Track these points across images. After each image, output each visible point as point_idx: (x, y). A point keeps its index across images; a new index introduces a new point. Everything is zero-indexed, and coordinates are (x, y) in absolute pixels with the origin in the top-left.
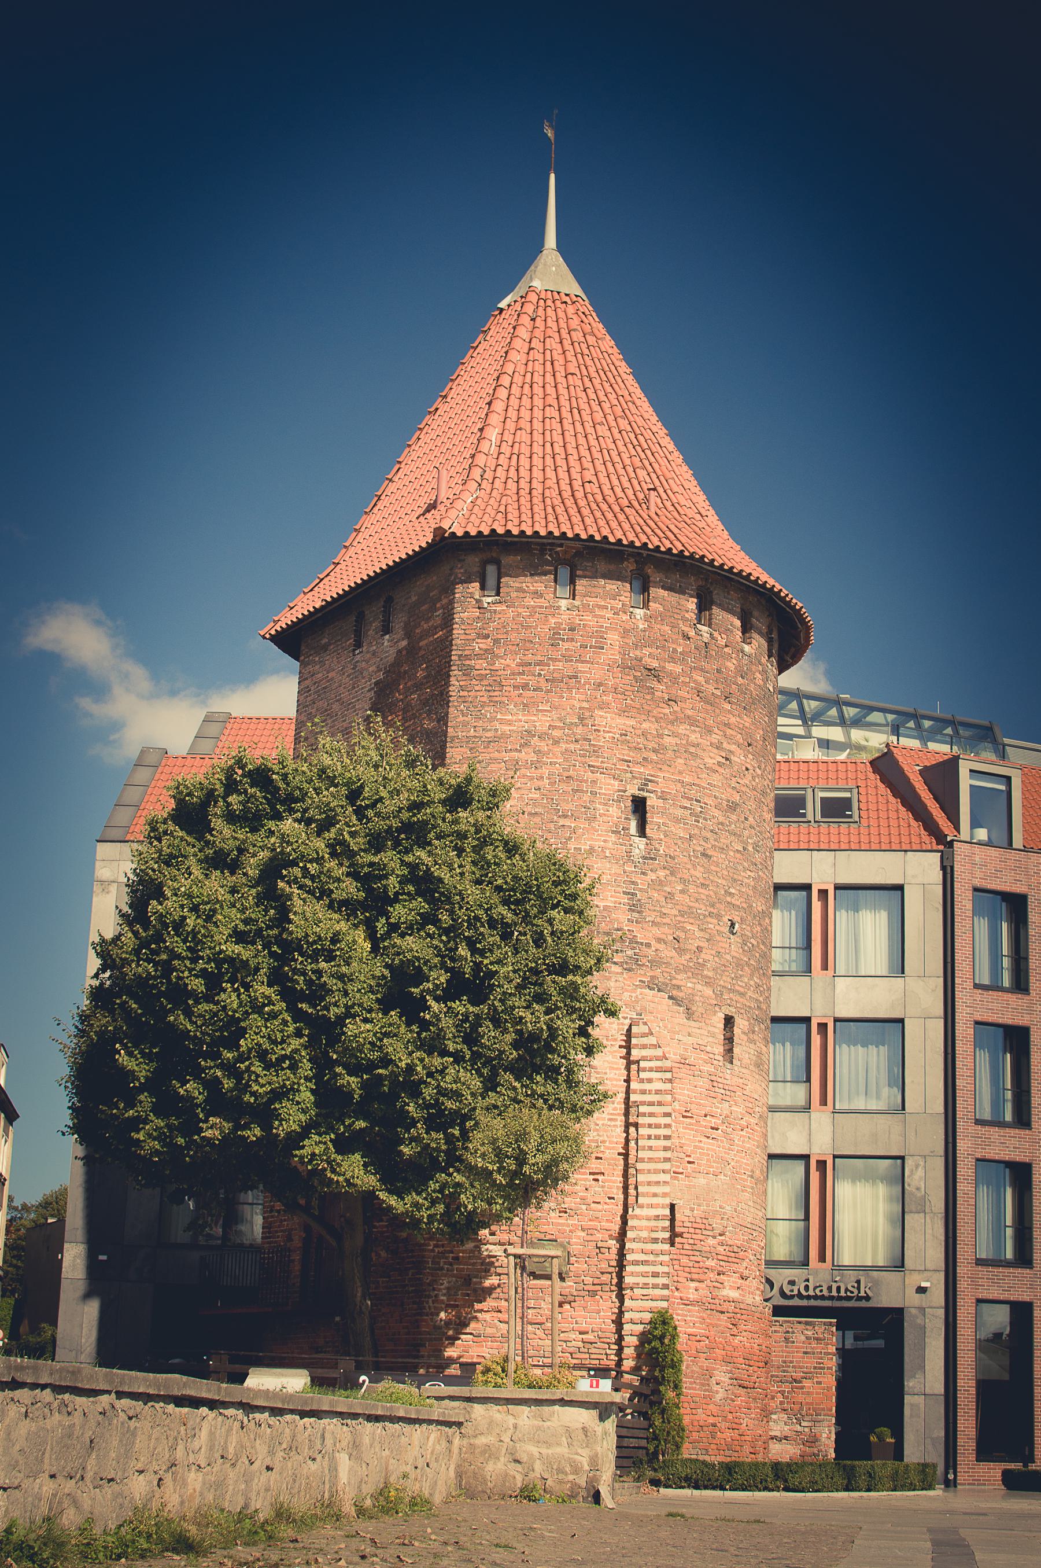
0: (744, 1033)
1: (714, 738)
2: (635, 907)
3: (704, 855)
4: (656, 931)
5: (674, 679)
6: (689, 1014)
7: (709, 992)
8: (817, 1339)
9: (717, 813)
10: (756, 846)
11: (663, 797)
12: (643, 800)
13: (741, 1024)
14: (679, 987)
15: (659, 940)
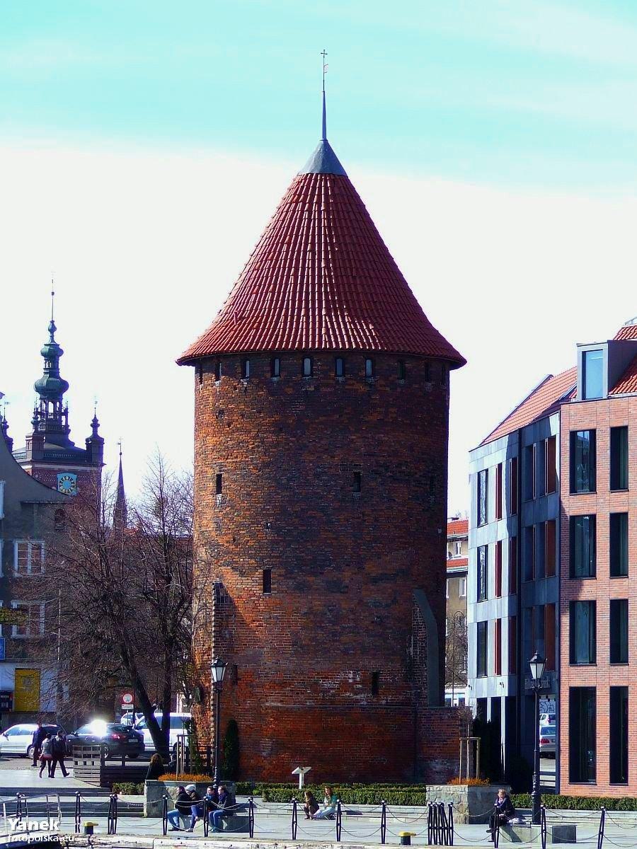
0: (280, 576)
1: (253, 434)
2: (218, 528)
3: (247, 494)
4: (226, 538)
5: (231, 411)
6: (242, 574)
7: (253, 561)
8: (452, 717)
9: (255, 471)
10: (289, 480)
11: (227, 472)
12: (221, 475)
13: (275, 573)
14: (236, 563)
15: (227, 542)
